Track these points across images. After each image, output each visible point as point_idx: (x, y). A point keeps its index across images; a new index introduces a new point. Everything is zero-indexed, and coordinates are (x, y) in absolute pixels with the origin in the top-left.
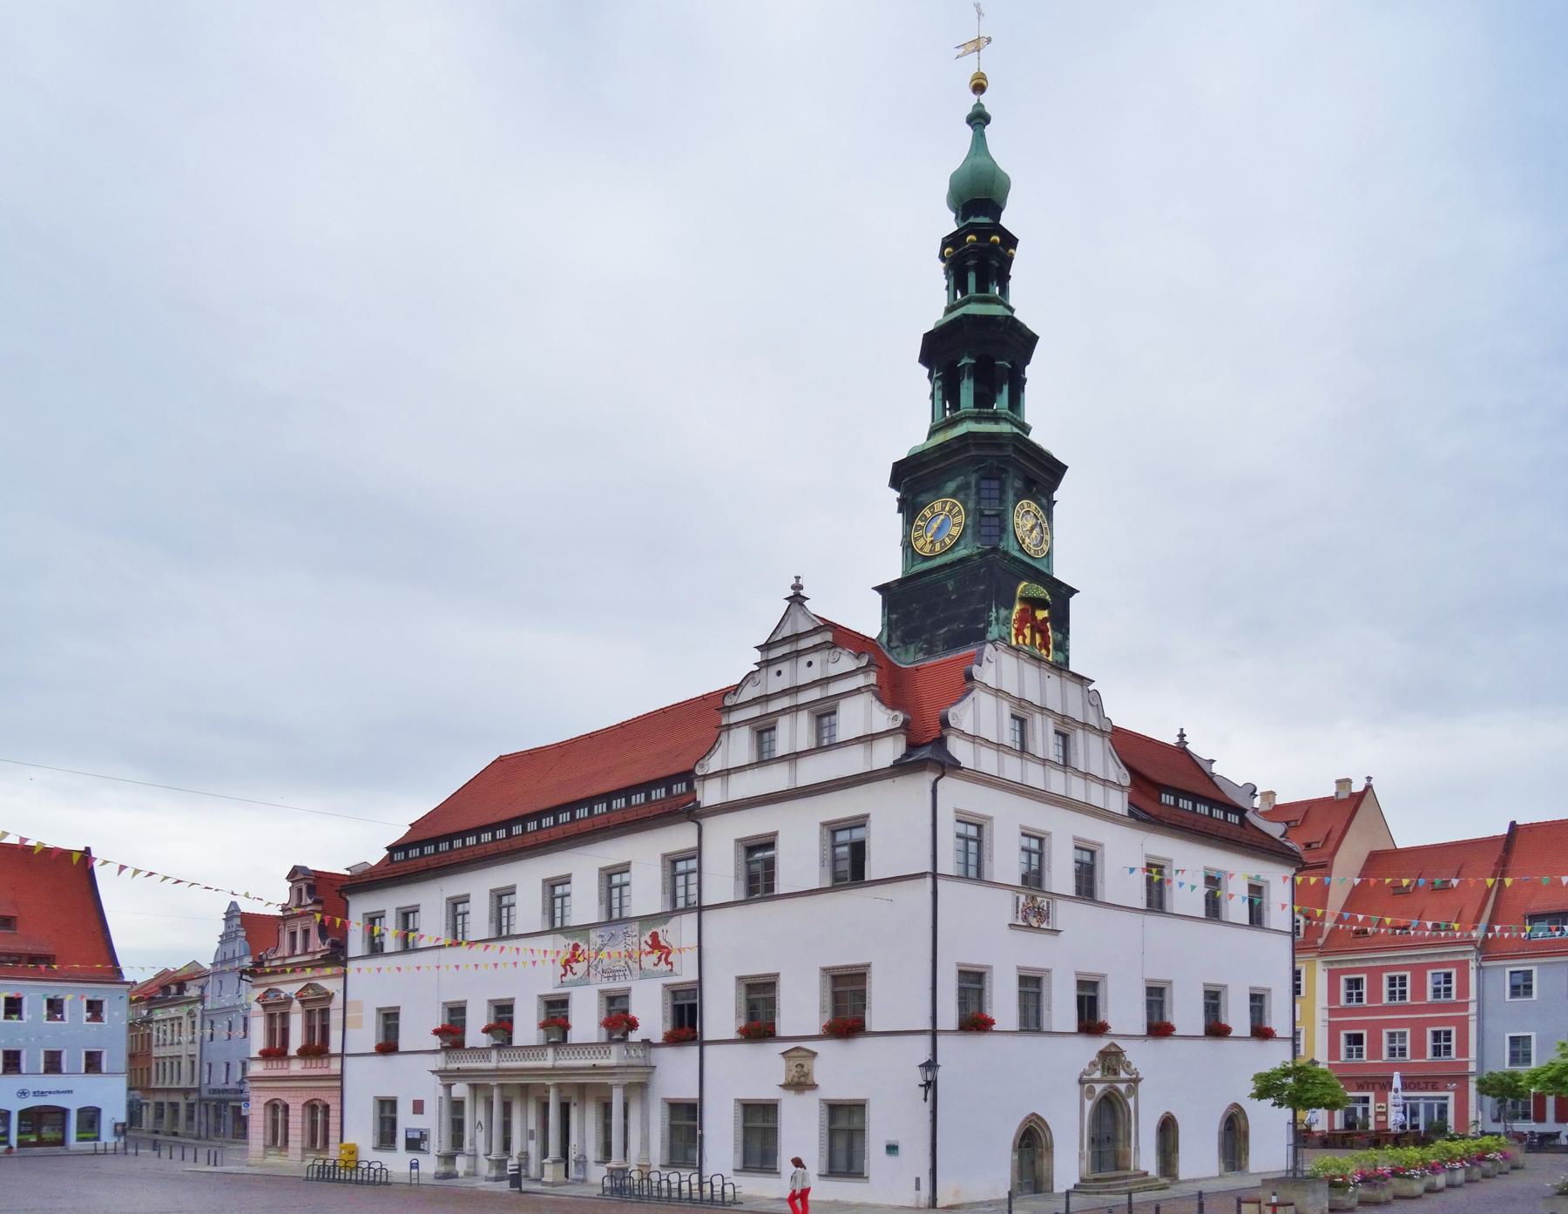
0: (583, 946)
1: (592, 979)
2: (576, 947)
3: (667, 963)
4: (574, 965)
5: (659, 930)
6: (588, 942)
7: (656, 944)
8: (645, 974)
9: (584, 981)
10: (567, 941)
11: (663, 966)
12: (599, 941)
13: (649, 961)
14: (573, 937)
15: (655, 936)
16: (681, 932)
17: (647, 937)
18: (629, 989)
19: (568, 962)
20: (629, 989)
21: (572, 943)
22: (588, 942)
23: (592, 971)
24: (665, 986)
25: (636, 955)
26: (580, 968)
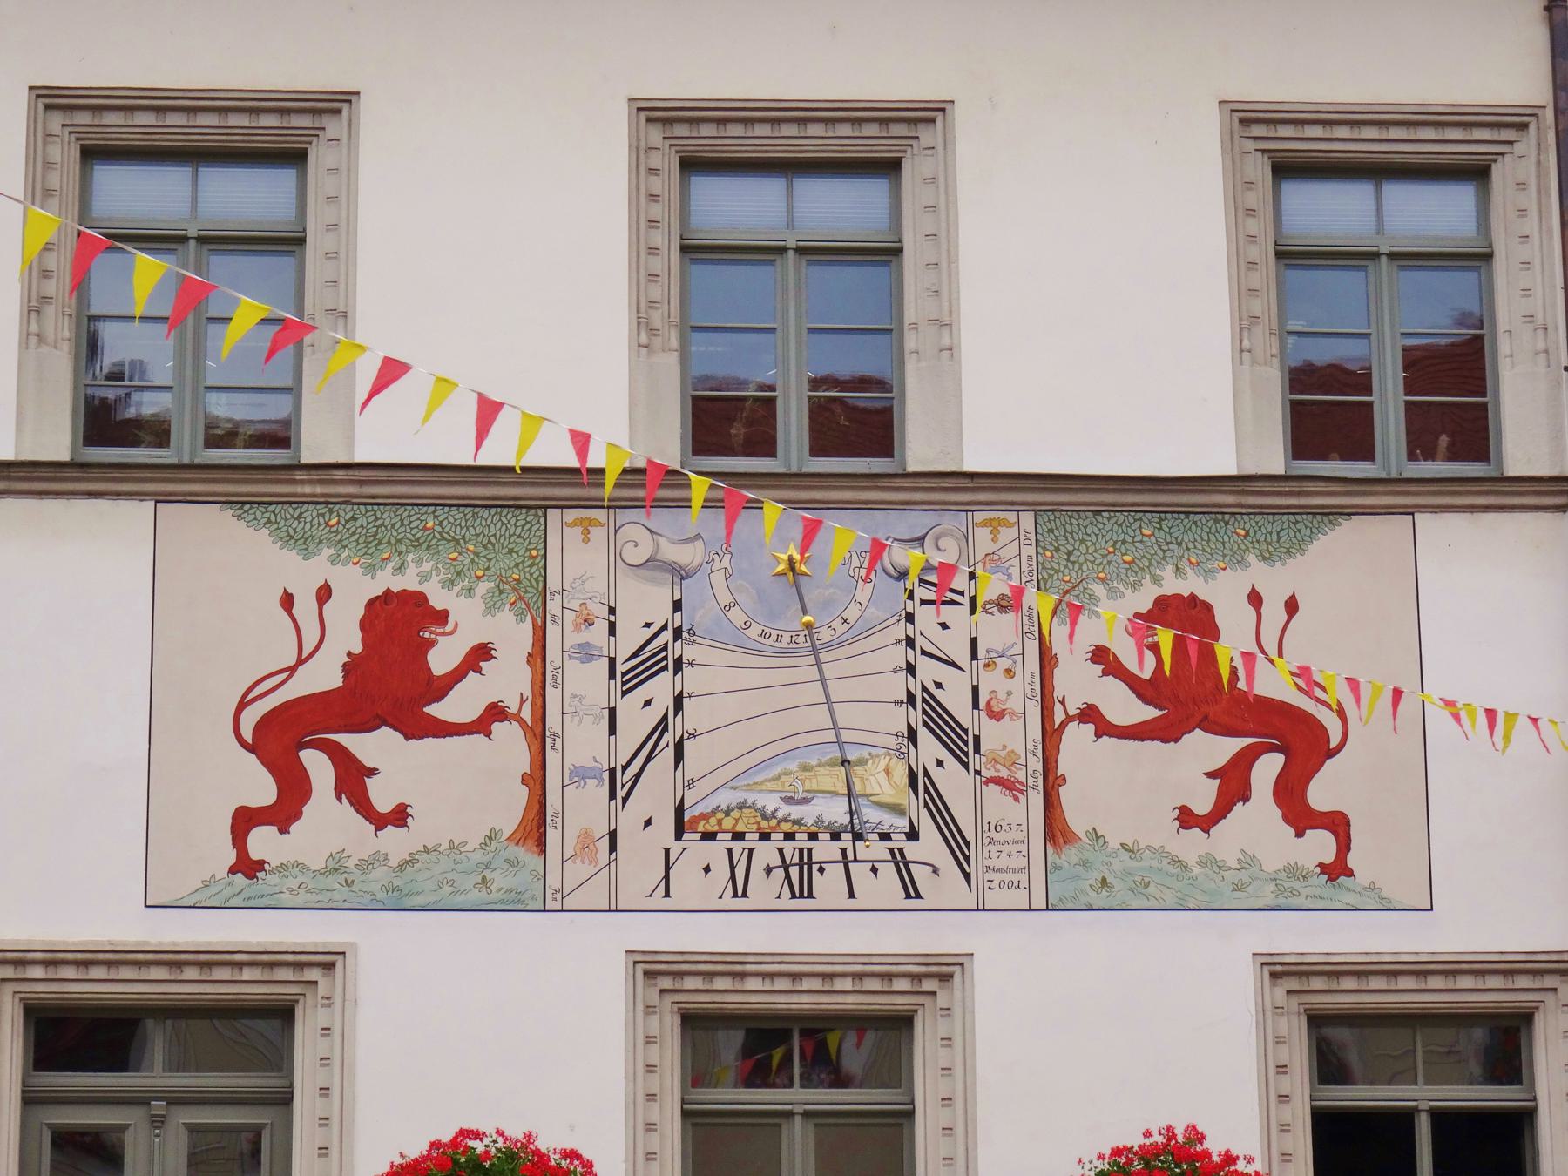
0: (470, 616)
1: (564, 860)
2: (399, 623)
3: (1300, 817)
4: (375, 747)
5: (1224, 594)
6: (532, 597)
10: (303, 574)
13: (1134, 787)
14: (371, 548)
17: (1111, 619)
18: (943, 971)
19: (282, 736)
20: (943, 971)
21: (357, 588)
22: (532, 597)
23: (579, 809)
24: (1278, 970)
25: (1011, 738)
26: (443, 783)
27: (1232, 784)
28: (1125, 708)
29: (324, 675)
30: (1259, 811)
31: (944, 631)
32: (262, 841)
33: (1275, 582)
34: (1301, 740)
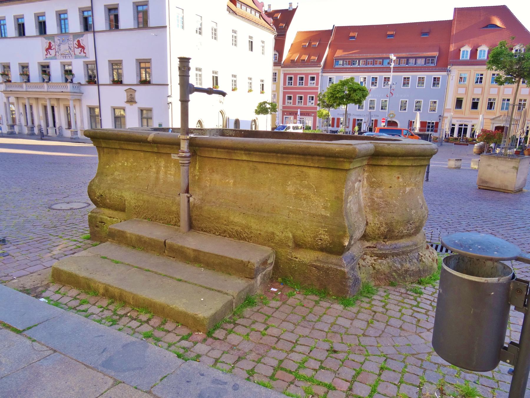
0: (53, 43)
1: (57, 57)
2: (50, 43)
3: (84, 53)
4: (50, 50)
5: (80, 39)
6: (54, 42)
7: (79, 46)
8: (76, 57)
9: (55, 58)
10: (46, 41)
11: (82, 54)
12: (58, 42)
13: (77, 51)
15: (79, 41)
16: (88, 39)
17: (76, 42)
21: (48, 42)
22: (54, 42)
23: (57, 53)
24: (84, 62)
26: (52, 52)
27: (81, 51)
28: (77, 47)
29: (48, 47)
30: (82, 52)
31: (70, 42)
32: (47, 56)
33: (82, 38)
34: (83, 48)
